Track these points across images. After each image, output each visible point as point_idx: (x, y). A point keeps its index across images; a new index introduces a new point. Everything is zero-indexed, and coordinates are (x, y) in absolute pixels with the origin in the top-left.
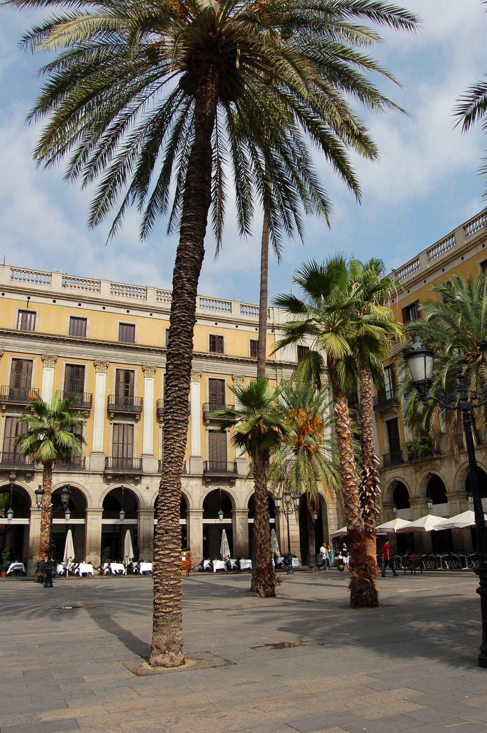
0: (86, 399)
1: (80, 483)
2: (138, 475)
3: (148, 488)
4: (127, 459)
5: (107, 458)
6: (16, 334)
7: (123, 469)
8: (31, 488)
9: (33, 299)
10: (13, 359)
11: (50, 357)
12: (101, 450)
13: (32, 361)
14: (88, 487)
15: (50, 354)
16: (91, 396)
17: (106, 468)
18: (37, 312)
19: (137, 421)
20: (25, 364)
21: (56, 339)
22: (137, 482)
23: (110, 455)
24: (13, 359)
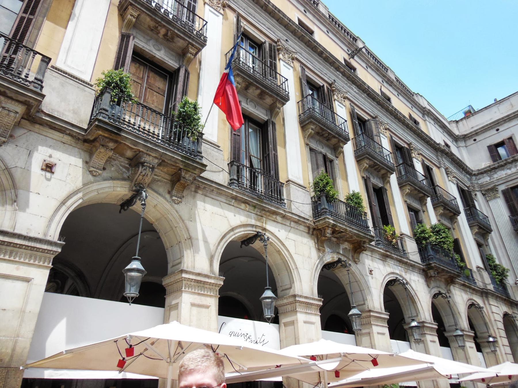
8: (183, 218)
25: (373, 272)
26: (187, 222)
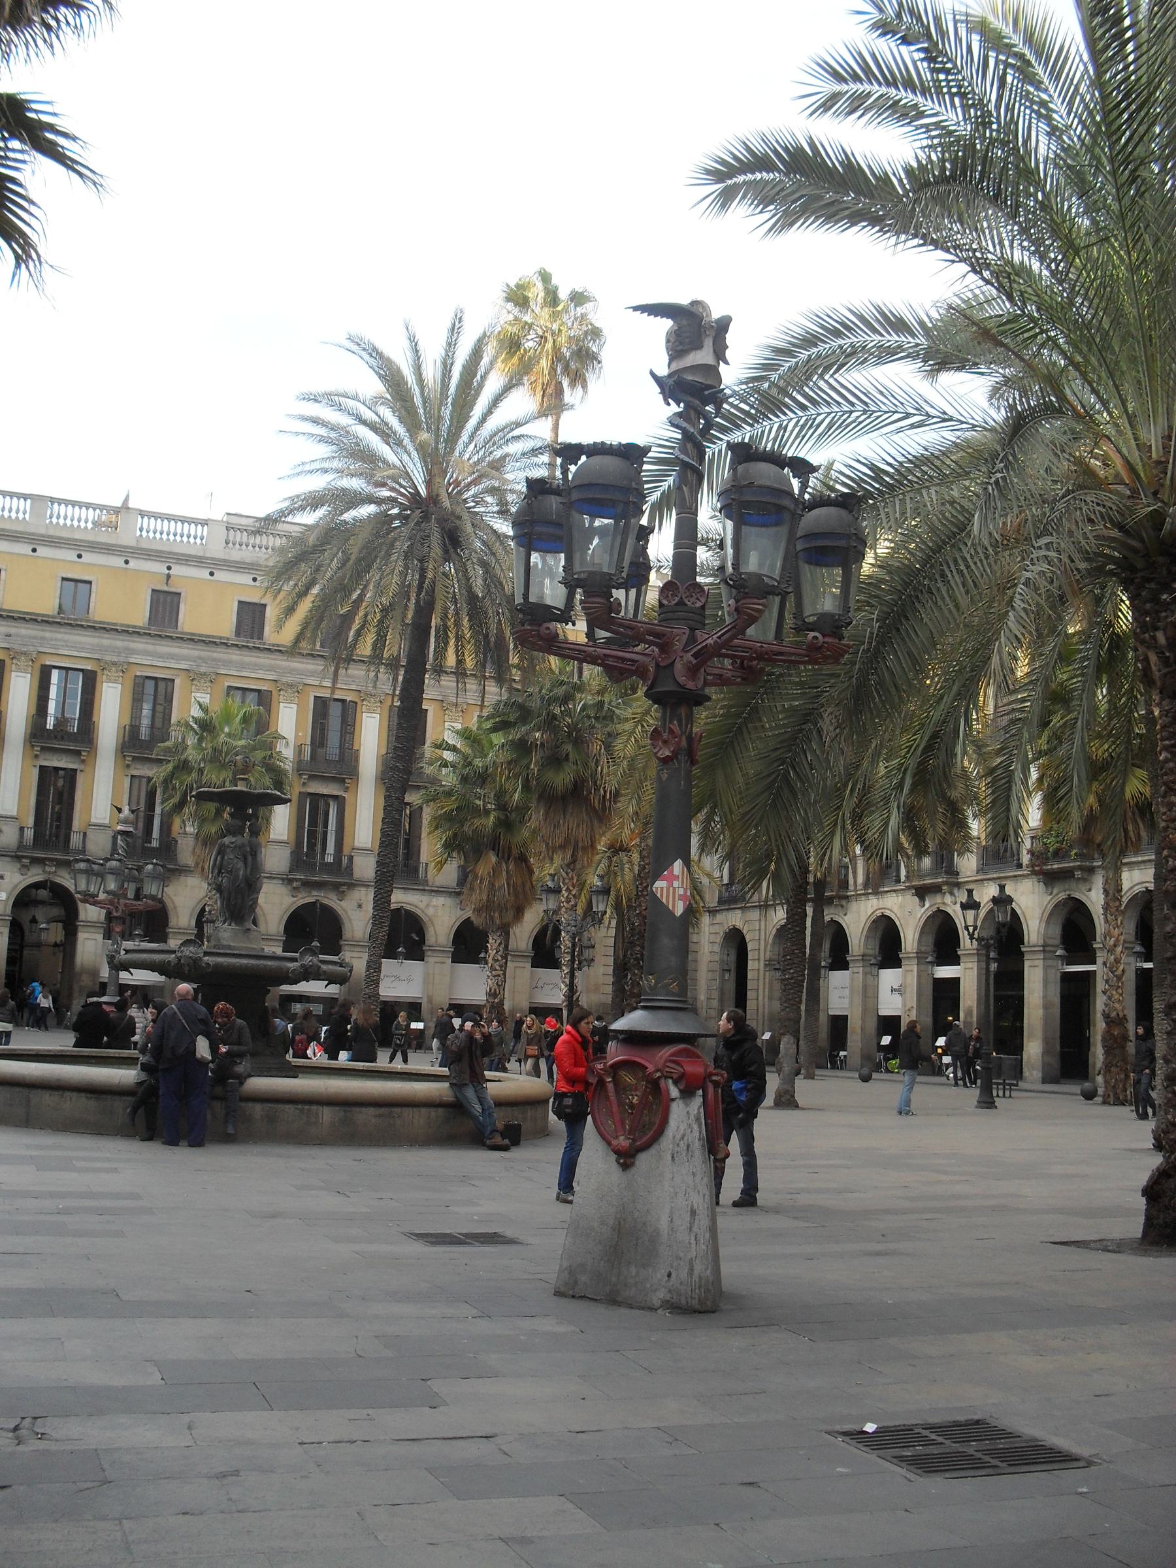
2: (345, 884)
3: (360, 906)
9: (177, 570)
11: (204, 675)
15: (203, 670)
18: (183, 595)
19: (346, 789)
22: (342, 896)
25: (364, 906)
26: (173, 898)
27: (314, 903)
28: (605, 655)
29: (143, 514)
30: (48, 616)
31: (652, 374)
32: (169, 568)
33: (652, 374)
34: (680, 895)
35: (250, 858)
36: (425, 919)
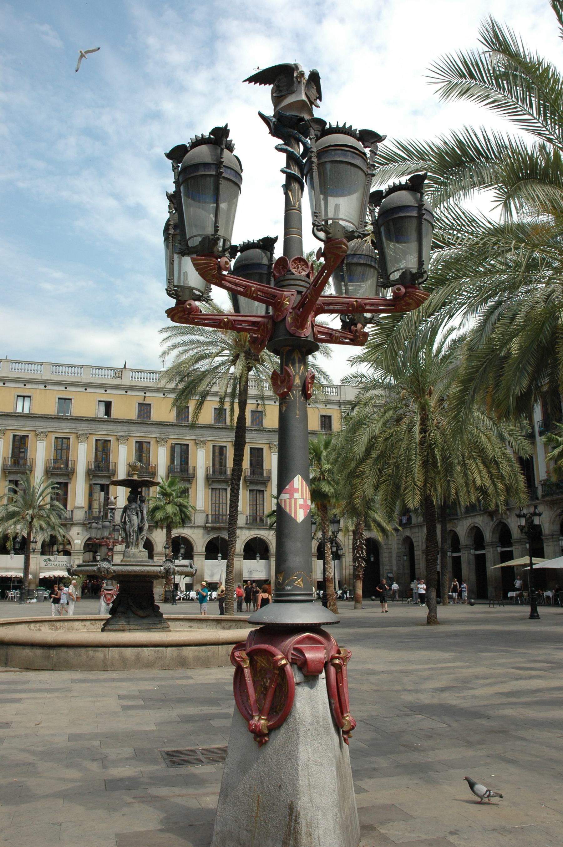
0: (190, 471)
1: (188, 534)
4: (222, 515)
5: (207, 515)
6: (138, 423)
7: (219, 522)
10: (137, 442)
11: (162, 439)
12: (203, 509)
13: (149, 443)
14: (194, 536)
15: (163, 437)
16: (195, 467)
17: (207, 522)
20: (145, 445)
21: (167, 425)
23: (210, 512)
24: (137, 442)
27: (218, 537)
28: (235, 321)
29: (133, 371)
30: (93, 418)
31: (261, 115)
32: (145, 393)
33: (261, 115)
34: (300, 505)
35: (140, 514)
36: (267, 541)
